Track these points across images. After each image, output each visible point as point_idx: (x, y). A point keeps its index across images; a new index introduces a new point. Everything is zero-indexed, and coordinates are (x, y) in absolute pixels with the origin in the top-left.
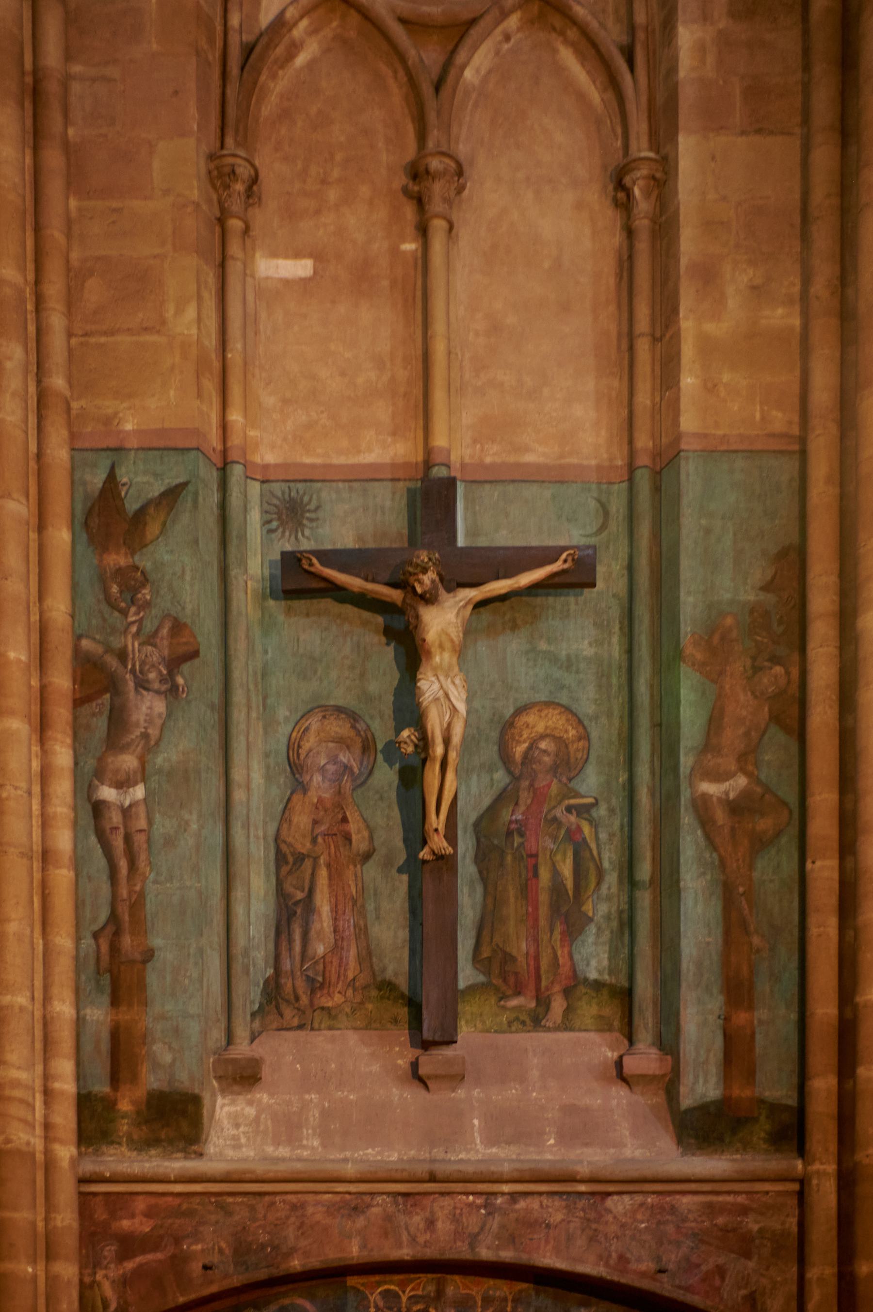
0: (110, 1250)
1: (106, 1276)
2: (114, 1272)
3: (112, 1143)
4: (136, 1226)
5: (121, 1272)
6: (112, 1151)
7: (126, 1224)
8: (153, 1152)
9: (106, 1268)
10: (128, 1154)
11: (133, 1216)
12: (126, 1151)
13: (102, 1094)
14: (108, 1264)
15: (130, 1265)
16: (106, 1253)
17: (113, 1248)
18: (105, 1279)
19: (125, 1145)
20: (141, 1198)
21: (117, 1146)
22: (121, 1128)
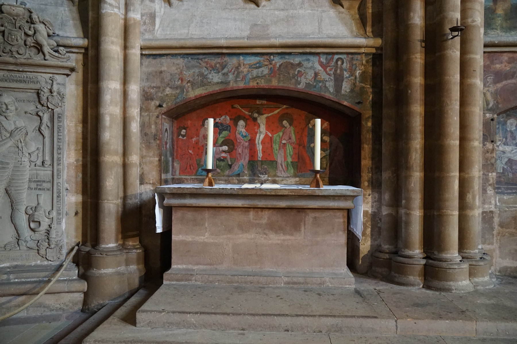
0: (490, 79)
1: (488, 90)
2: (492, 89)
3: (493, 29)
4: (503, 67)
5: (496, 88)
6: (493, 33)
7: (498, 66)
8: (513, 33)
9: (488, 87)
10: (501, 34)
11: (502, 63)
12: (500, 32)
13: (489, 7)
14: (489, 85)
15: (499, 85)
16: (488, 80)
17: (491, 78)
18: (488, 92)
19: (499, 29)
20: (505, 54)
21: (495, 30)
22: (497, 22)
